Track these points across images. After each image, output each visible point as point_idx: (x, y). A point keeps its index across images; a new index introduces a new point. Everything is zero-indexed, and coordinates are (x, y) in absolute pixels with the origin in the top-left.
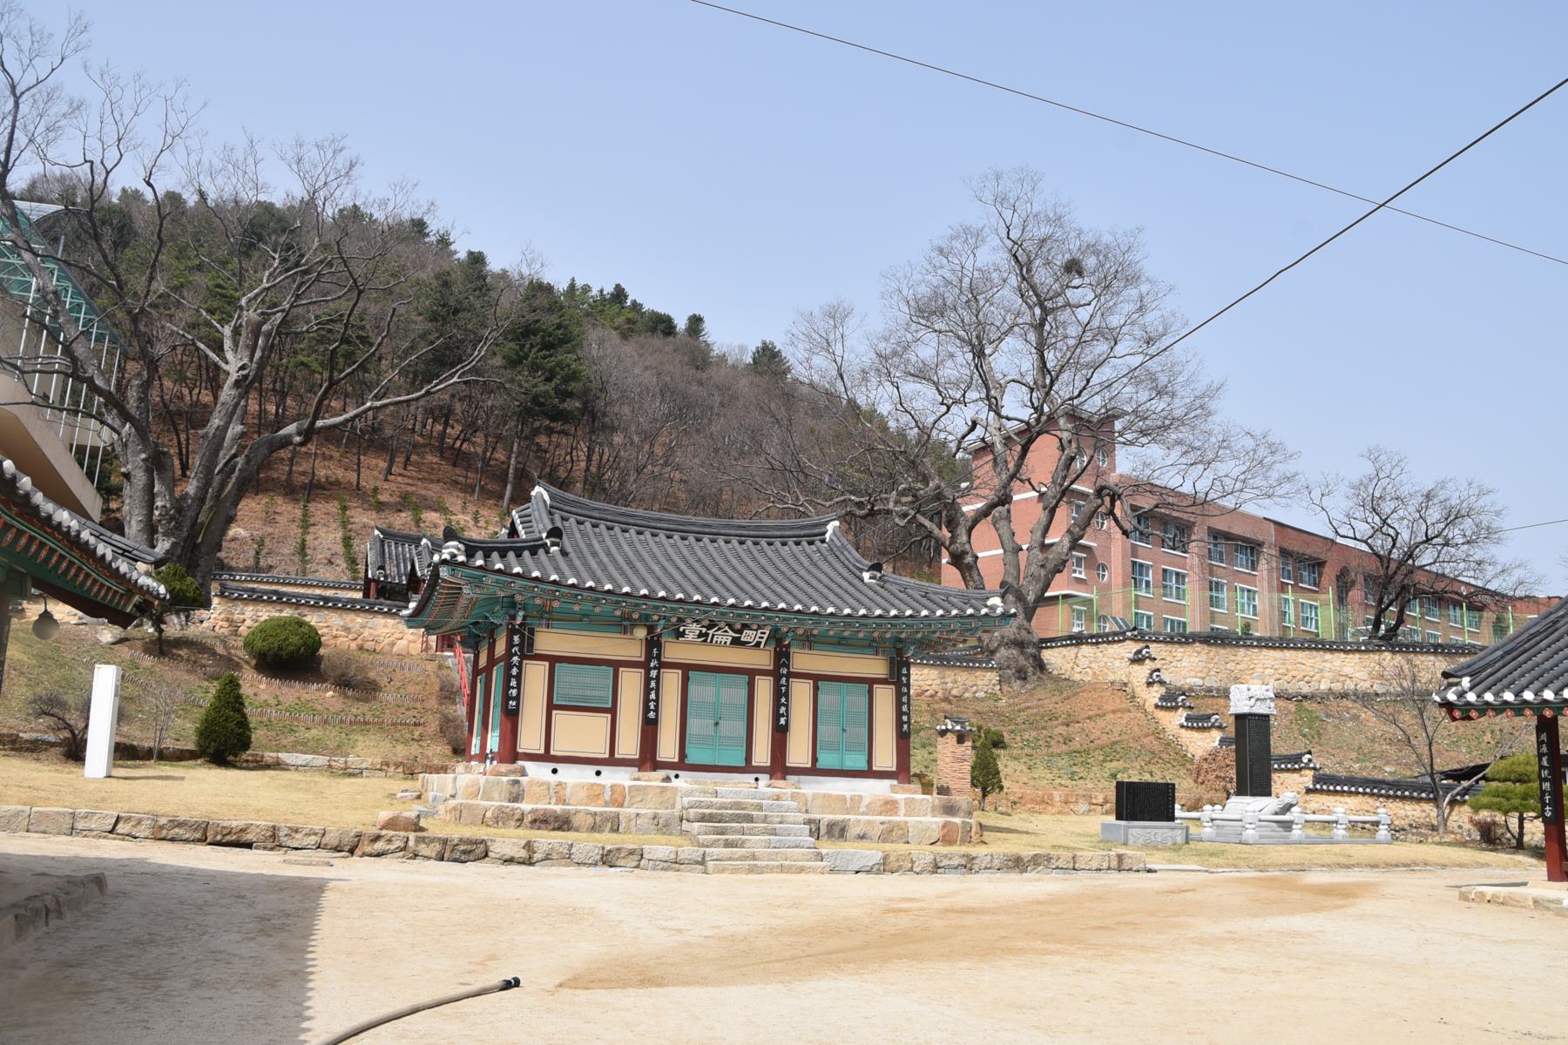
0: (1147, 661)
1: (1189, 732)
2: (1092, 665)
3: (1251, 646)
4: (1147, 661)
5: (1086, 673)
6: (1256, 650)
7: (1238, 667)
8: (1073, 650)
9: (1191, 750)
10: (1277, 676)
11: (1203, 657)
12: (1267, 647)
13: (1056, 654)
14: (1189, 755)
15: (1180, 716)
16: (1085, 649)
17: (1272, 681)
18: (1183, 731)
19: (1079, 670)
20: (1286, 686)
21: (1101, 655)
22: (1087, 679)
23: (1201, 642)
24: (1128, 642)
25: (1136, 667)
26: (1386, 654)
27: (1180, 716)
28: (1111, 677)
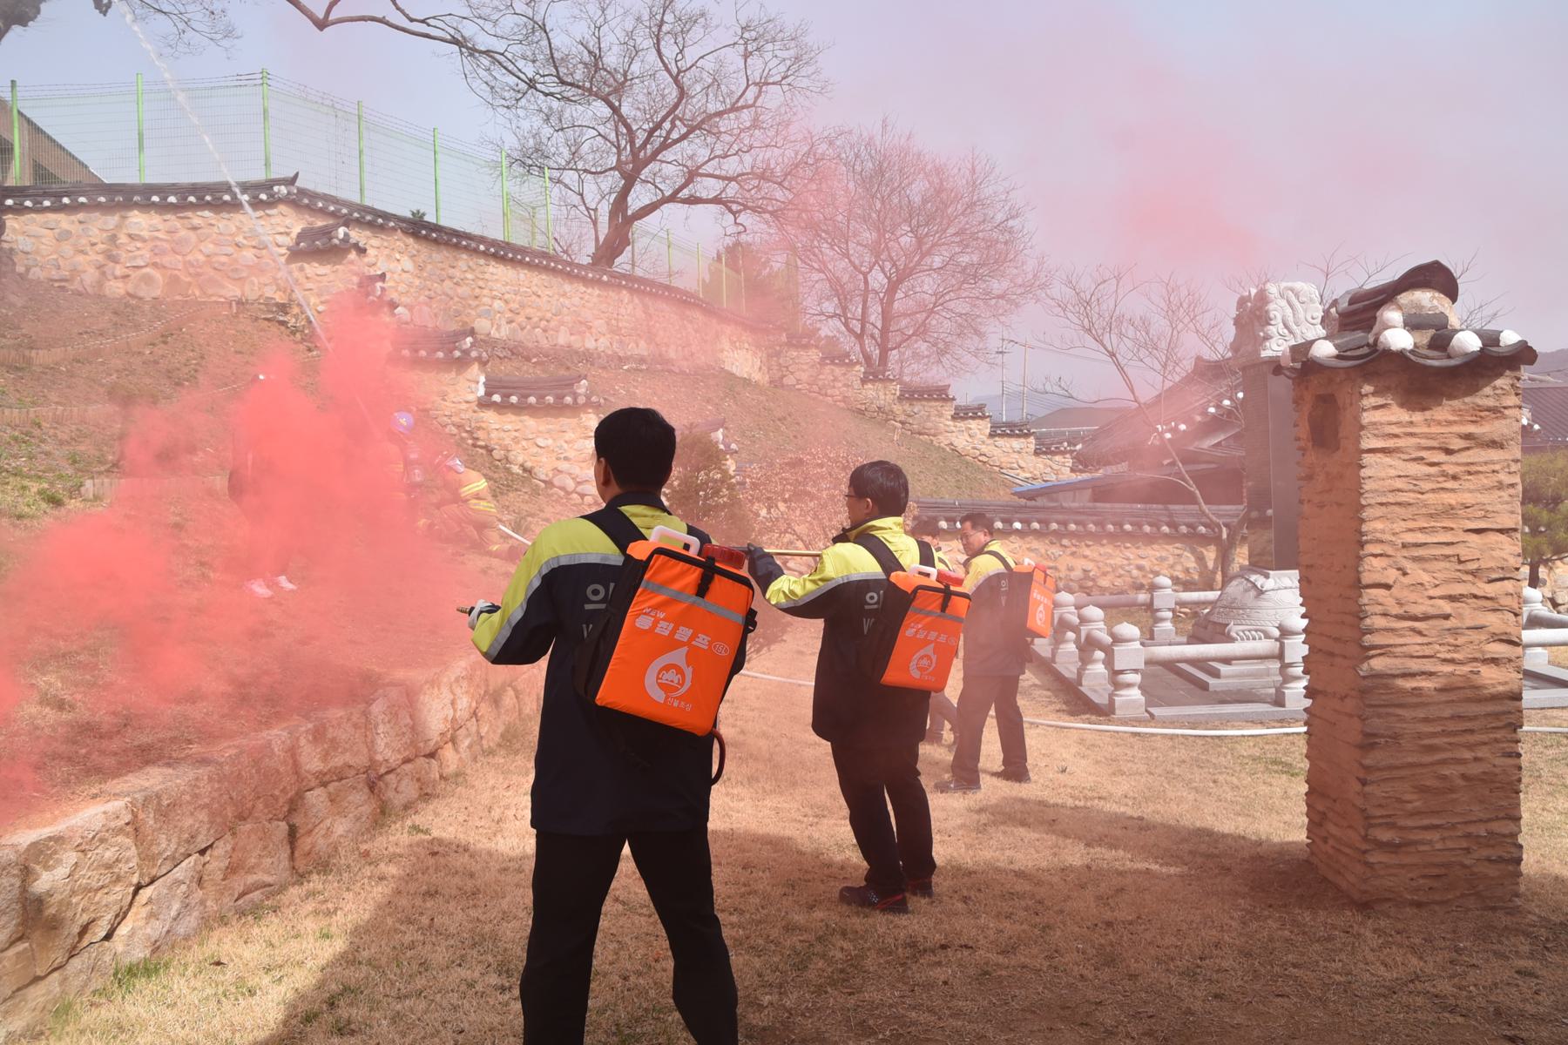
0: (353, 255)
1: (511, 417)
2: (167, 260)
3: (476, 251)
4: (353, 255)
5: (148, 280)
6: (482, 261)
7: (460, 290)
8: (112, 220)
9: (519, 456)
10: (509, 315)
11: (408, 264)
12: (495, 256)
13: (34, 229)
14: (516, 469)
15: (474, 383)
16: (139, 221)
17: (503, 322)
18: (490, 417)
19: (119, 271)
20: (521, 335)
21: (192, 236)
22: (147, 293)
23: (405, 232)
24: (282, 208)
25: (313, 268)
26: (624, 292)
27: (474, 383)
28: (233, 291)
